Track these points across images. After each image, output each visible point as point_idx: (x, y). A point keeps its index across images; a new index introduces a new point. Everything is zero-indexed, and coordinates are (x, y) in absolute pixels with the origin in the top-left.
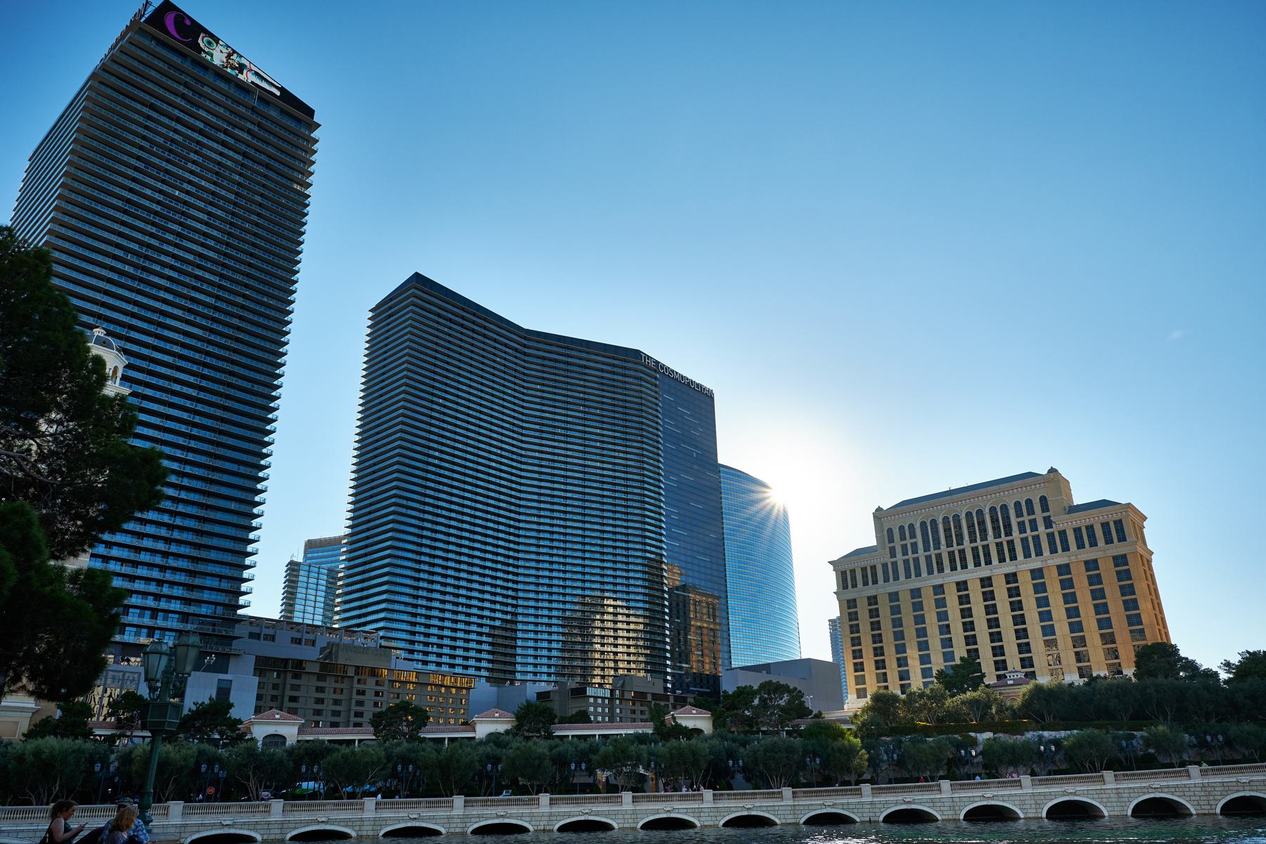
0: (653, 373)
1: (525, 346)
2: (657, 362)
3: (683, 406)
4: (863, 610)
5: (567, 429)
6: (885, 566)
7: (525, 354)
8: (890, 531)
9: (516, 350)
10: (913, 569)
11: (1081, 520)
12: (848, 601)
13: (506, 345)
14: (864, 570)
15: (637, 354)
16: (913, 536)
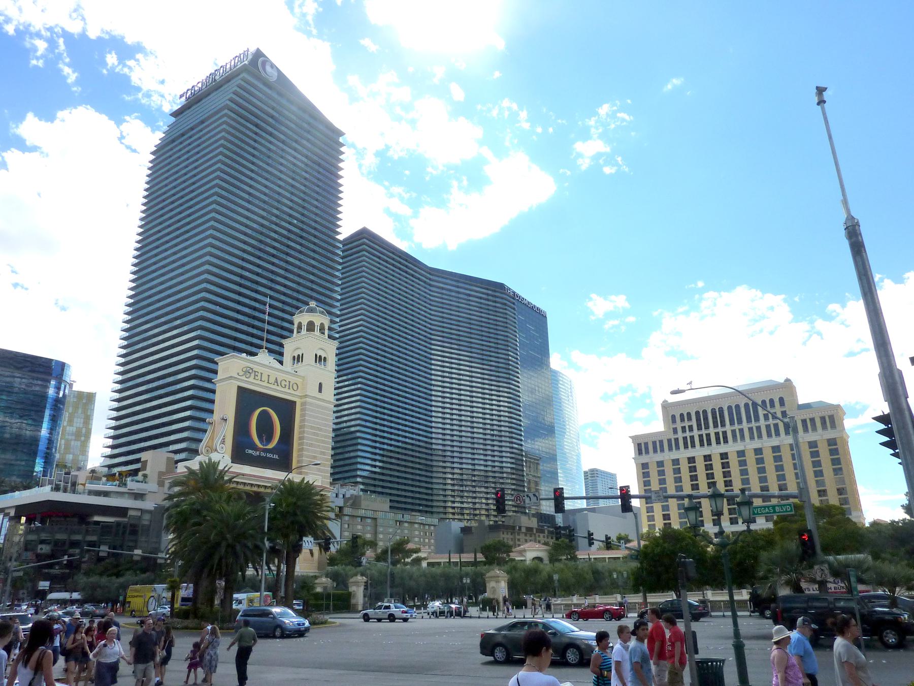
0: (512, 300)
1: (430, 279)
2: (514, 293)
3: (530, 325)
4: (653, 471)
5: (459, 340)
6: (669, 441)
7: (430, 285)
8: (673, 417)
9: (425, 282)
10: (689, 443)
11: (807, 416)
12: (643, 464)
13: (413, 276)
14: (654, 443)
15: (501, 287)
16: (690, 419)
